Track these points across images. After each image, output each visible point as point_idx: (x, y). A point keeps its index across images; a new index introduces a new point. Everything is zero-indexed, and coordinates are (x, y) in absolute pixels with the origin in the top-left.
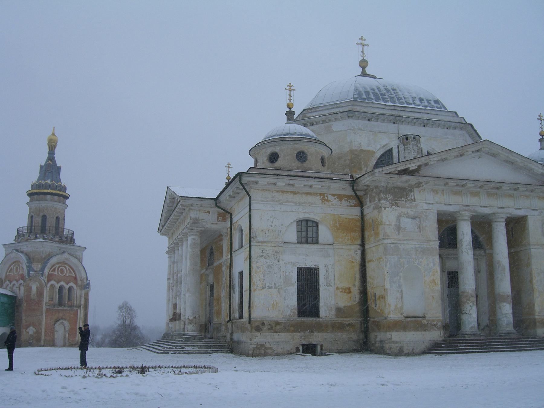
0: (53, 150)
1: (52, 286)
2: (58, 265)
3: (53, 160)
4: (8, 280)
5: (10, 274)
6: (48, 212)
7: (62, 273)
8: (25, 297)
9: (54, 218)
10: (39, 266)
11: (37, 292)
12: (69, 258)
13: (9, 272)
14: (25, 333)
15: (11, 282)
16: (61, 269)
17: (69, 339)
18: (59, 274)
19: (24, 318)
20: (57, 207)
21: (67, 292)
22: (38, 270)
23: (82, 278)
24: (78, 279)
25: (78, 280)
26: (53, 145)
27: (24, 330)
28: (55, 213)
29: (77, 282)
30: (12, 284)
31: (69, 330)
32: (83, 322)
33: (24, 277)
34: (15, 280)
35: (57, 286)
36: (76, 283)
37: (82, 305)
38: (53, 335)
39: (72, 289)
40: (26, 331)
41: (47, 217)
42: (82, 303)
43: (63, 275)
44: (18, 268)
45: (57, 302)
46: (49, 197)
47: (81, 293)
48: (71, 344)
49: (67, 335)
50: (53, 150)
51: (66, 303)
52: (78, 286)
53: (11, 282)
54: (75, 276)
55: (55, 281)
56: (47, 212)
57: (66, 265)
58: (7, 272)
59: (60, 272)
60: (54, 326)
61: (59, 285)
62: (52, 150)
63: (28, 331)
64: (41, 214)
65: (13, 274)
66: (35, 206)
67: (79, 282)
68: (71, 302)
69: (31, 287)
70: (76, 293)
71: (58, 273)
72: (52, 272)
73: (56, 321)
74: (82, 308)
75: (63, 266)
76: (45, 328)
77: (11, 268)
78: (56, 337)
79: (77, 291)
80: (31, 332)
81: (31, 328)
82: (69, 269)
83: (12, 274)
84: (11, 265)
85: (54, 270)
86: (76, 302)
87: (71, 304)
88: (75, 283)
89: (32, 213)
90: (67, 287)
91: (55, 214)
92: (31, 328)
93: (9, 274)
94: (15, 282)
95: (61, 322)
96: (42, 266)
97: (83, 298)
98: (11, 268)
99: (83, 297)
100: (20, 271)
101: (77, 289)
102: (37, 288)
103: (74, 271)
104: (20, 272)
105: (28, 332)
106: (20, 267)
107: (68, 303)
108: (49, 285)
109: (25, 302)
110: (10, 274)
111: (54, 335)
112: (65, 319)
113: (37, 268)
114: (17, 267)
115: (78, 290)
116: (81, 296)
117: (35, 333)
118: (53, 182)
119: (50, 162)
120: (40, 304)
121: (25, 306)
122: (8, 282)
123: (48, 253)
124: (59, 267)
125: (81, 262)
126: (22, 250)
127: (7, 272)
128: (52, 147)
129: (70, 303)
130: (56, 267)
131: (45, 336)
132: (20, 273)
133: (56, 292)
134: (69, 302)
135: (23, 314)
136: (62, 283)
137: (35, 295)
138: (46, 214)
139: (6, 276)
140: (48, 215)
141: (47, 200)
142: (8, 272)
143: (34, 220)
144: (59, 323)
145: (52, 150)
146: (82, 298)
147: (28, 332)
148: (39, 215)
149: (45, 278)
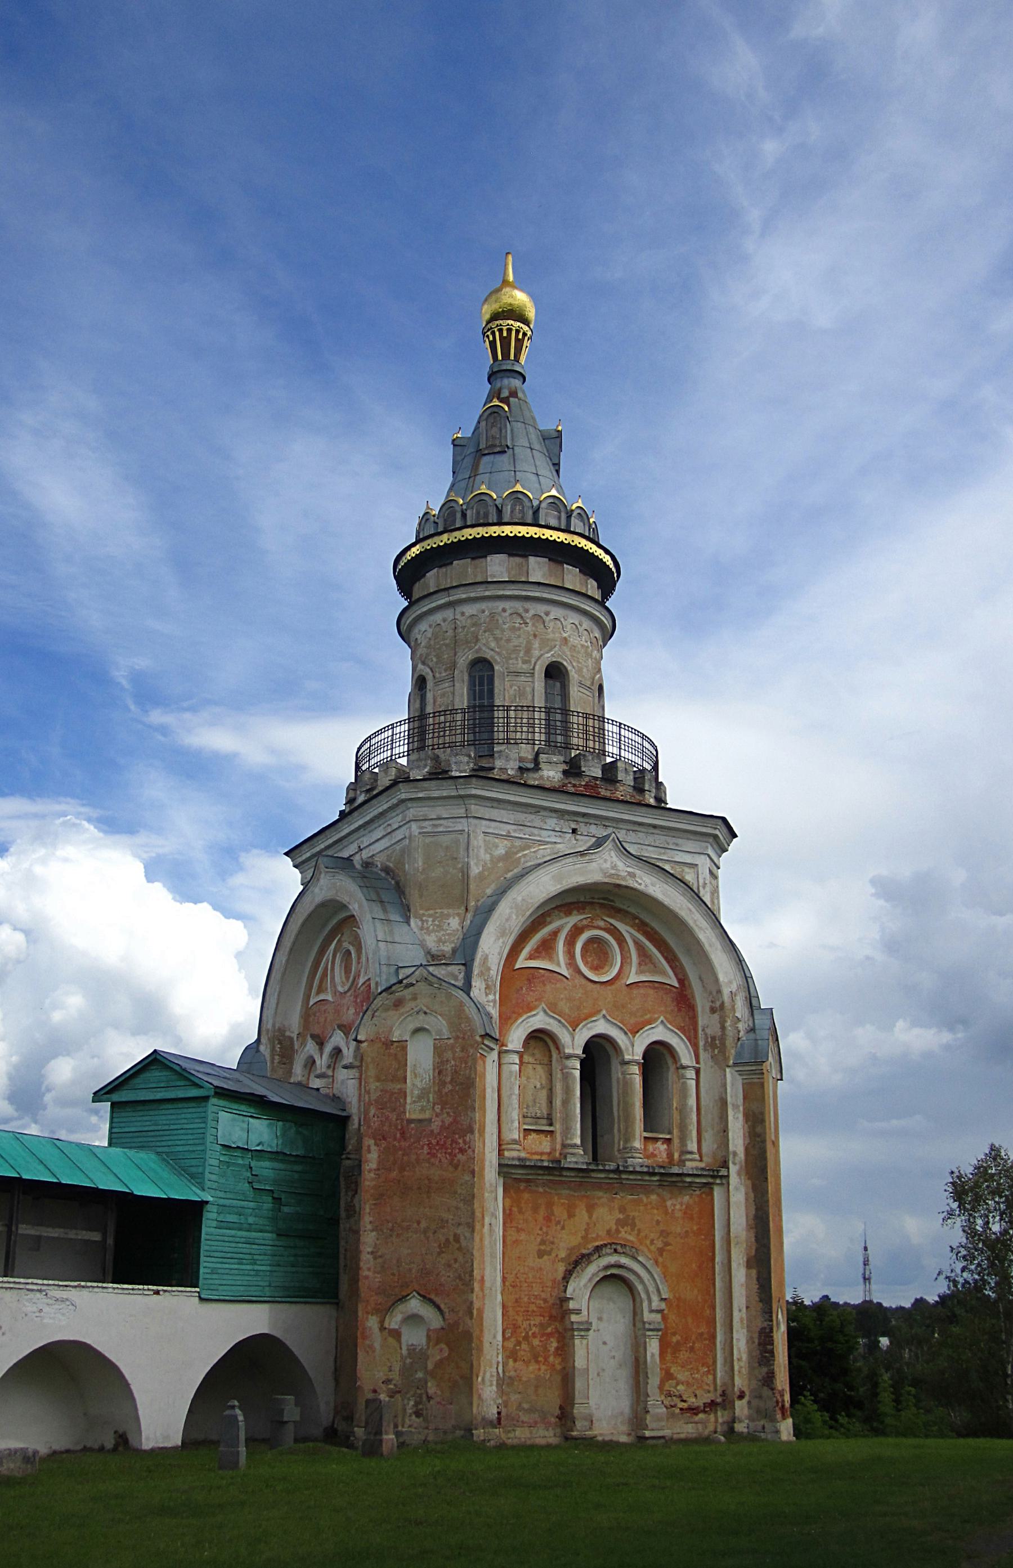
0: (512, 357)
1: (539, 1038)
2: (571, 921)
3: (511, 399)
5: (321, 997)
6: (497, 639)
7: (596, 968)
8: (372, 1111)
9: (534, 669)
10: (454, 923)
11: (439, 1069)
12: (632, 875)
14: (377, 1339)
15: (321, 1044)
16: (591, 940)
17: (668, 1376)
18: (579, 972)
19: (369, 1239)
20: (547, 614)
21: (638, 1081)
22: (447, 948)
23: (719, 992)
24: (701, 1003)
25: (699, 1009)
26: (509, 330)
27: (372, 1322)
28: (536, 644)
29: (694, 1019)
30: (328, 1049)
31: (664, 1318)
32: (749, 1265)
34: (340, 1027)
35: (574, 1043)
36: (690, 1031)
37: (735, 1154)
38: (557, 1349)
39: (670, 1061)
40: (382, 1322)
41: (496, 668)
42: (731, 1148)
43: (605, 978)
45: (578, 1141)
46: (498, 566)
47: (724, 1085)
48: (685, 1405)
49: (653, 1347)
50: (512, 357)
51: (637, 1144)
52: (701, 1043)
53: (321, 1044)
54: (681, 981)
55: (553, 1008)
56: (493, 645)
57: (621, 921)
58: (307, 997)
59: (586, 964)
60: (565, 1291)
61: (583, 1035)
62: (506, 355)
63: (394, 1321)
64: (464, 658)
65: (335, 992)
66: (430, 626)
67: (705, 1020)
68: (668, 1141)
70: (693, 1082)
71: (572, 963)
72: (531, 957)
73: (577, 1262)
74: (734, 1180)
75: (602, 924)
76: (504, 1307)
77: (326, 969)
78: (579, 1363)
79: (698, 1071)
80: (414, 1337)
81: (415, 1305)
82: (637, 943)
83: (330, 998)
84: (322, 951)
85: (546, 948)
86: (699, 1142)
87: (670, 1155)
88: (682, 1029)
89: (420, 666)
90: (634, 1049)
91: (536, 653)
92: (415, 1305)
94: (338, 1039)
95: (607, 1267)
96: (467, 923)
97: (741, 1116)
98: (326, 969)
99: (735, 1107)
101: (698, 1062)
102: (439, 1050)
103: (672, 959)
105: (396, 1334)
107: (651, 1147)
108: (516, 1038)
109: (372, 1142)
110: (321, 997)
111: (565, 1350)
112: (630, 1250)
113: (440, 941)
114: (348, 952)
115: (702, 1066)
116: (723, 1103)
117: (436, 1337)
118: (518, 488)
119: (496, 402)
120: (462, 1151)
121: (373, 1165)
122: (311, 1047)
123: (501, 851)
124: (576, 931)
125: (707, 899)
126: (365, 854)
127: (307, 997)
128: (505, 342)
129: (662, 1147)
130: (555, 934)
131: (512, 1355)
133: (566, 1077)
134: (656, 1140)
135: (367, 1220)
136: (601, 1027)
137: (431, 1096)
138: (488, 655)
139: (307, 1015)
140: (497, 658)
141: (489, 580)
142: (314, 991)
143: (429, 696)
144: (593, 1270)
145: (506, 355)
146: (730, 1113)
147: (396, 1334)
148: (453, 666)
149: (487, 987)
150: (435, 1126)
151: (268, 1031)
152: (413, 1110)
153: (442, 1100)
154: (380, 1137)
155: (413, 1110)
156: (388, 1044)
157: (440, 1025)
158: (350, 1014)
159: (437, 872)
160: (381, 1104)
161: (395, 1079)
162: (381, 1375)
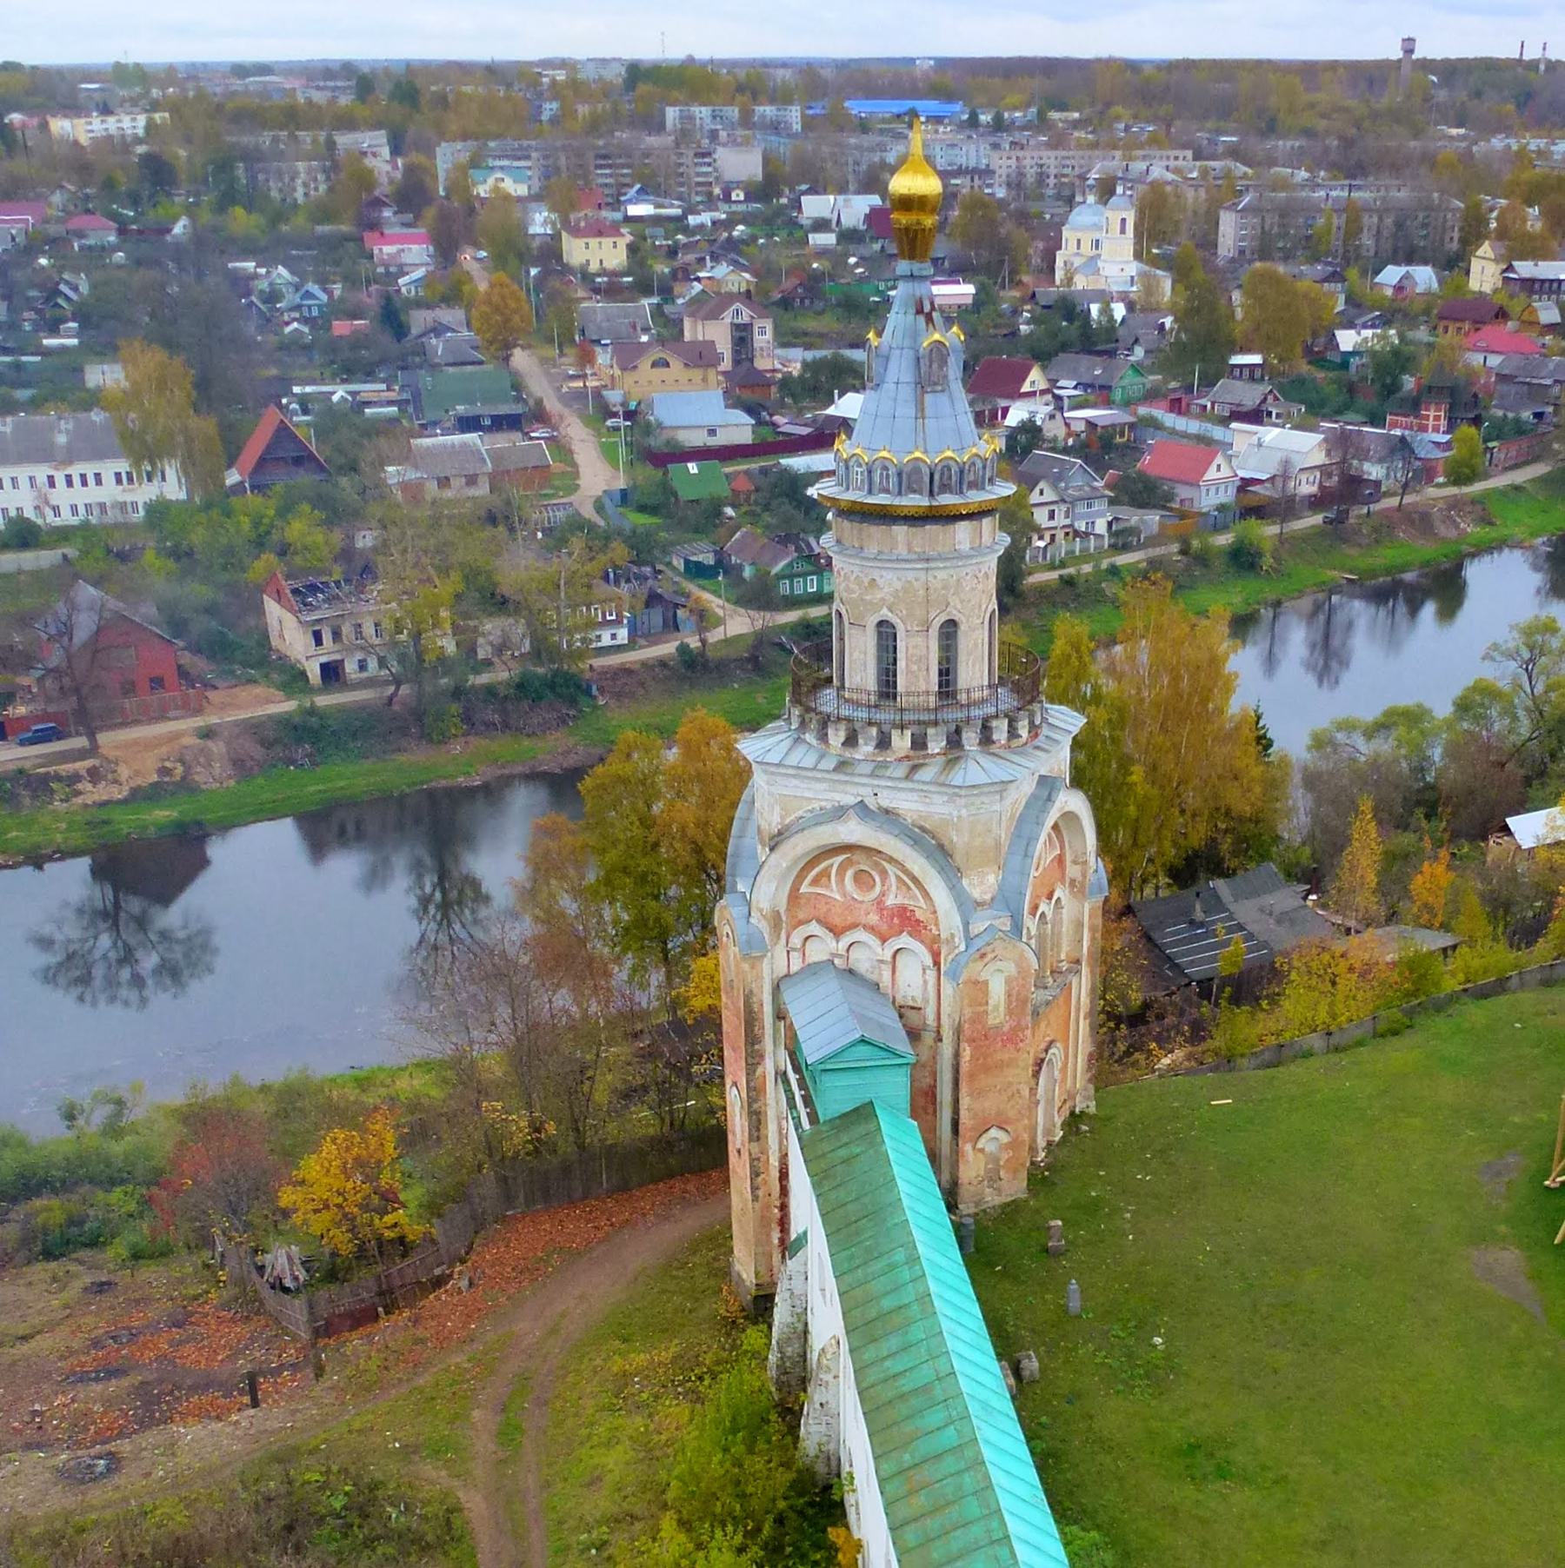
4: (819, 921)
13: (815, 882)
22: (988, 897)
33: (918, 921)
44: (877, 879)
63: (980, 1145)
69: (986, 983)
81: (994, 1132)
83: (838, 897)
92: (994, 1132)
93: (812, 890)
100: (883, 894)
102: (1008, 981)
104: (892, 896)
106: (884, 873)
132: (890, 901)
150: (1006, 1029)
151: (761, 911)
152: (992, 1021)
153: (1010, 1011)
154: (971, 1041)
155: (992, 1021)
156: (976, 983)
157: (1010, 968)
158: (873, 918)
159: (978, 842)
160: (973, 1021)
161: (980, 1005)
162: (973, 1174)
